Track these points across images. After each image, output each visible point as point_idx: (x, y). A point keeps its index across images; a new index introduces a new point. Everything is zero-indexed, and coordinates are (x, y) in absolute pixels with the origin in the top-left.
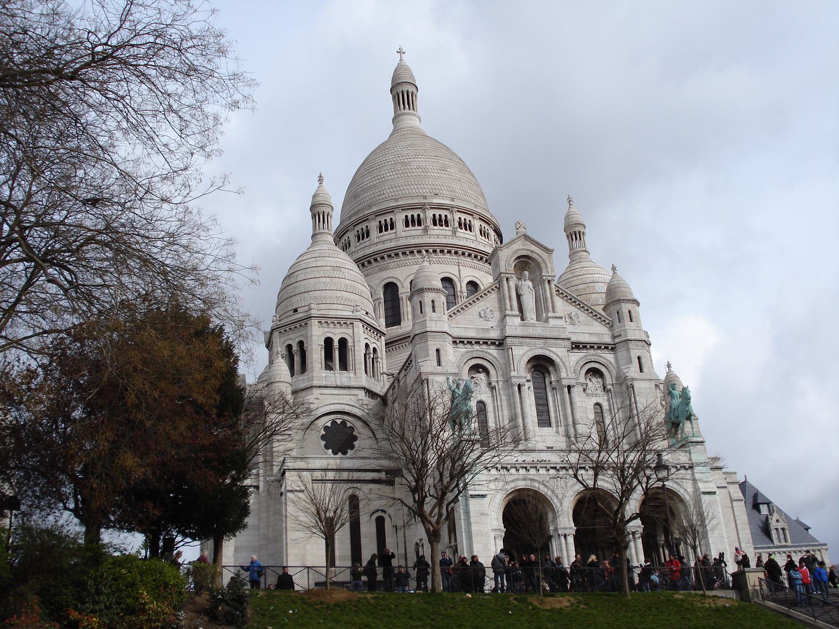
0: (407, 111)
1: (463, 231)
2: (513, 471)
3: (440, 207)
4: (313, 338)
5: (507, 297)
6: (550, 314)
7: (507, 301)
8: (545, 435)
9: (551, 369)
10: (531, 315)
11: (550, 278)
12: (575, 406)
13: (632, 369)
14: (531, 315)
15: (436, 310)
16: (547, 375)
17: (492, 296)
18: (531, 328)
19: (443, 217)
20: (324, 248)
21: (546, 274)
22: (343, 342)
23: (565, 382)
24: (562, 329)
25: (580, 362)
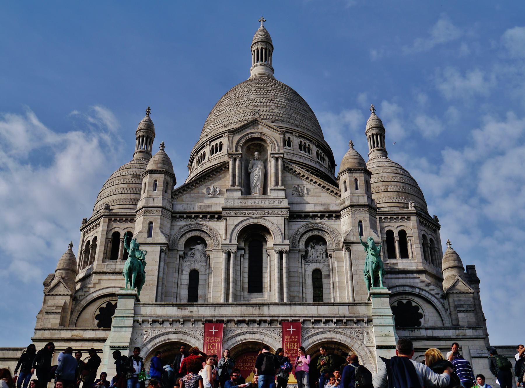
0: (259, 63)
2: (167, 325)
10: (257, 191)
11: (276, 156)
13: (352, 234)
16: (264, 244)
17: (221, 176)
18: (249, 200)
21: (274, 152)
24: (281, 200)
25: (301, 230)
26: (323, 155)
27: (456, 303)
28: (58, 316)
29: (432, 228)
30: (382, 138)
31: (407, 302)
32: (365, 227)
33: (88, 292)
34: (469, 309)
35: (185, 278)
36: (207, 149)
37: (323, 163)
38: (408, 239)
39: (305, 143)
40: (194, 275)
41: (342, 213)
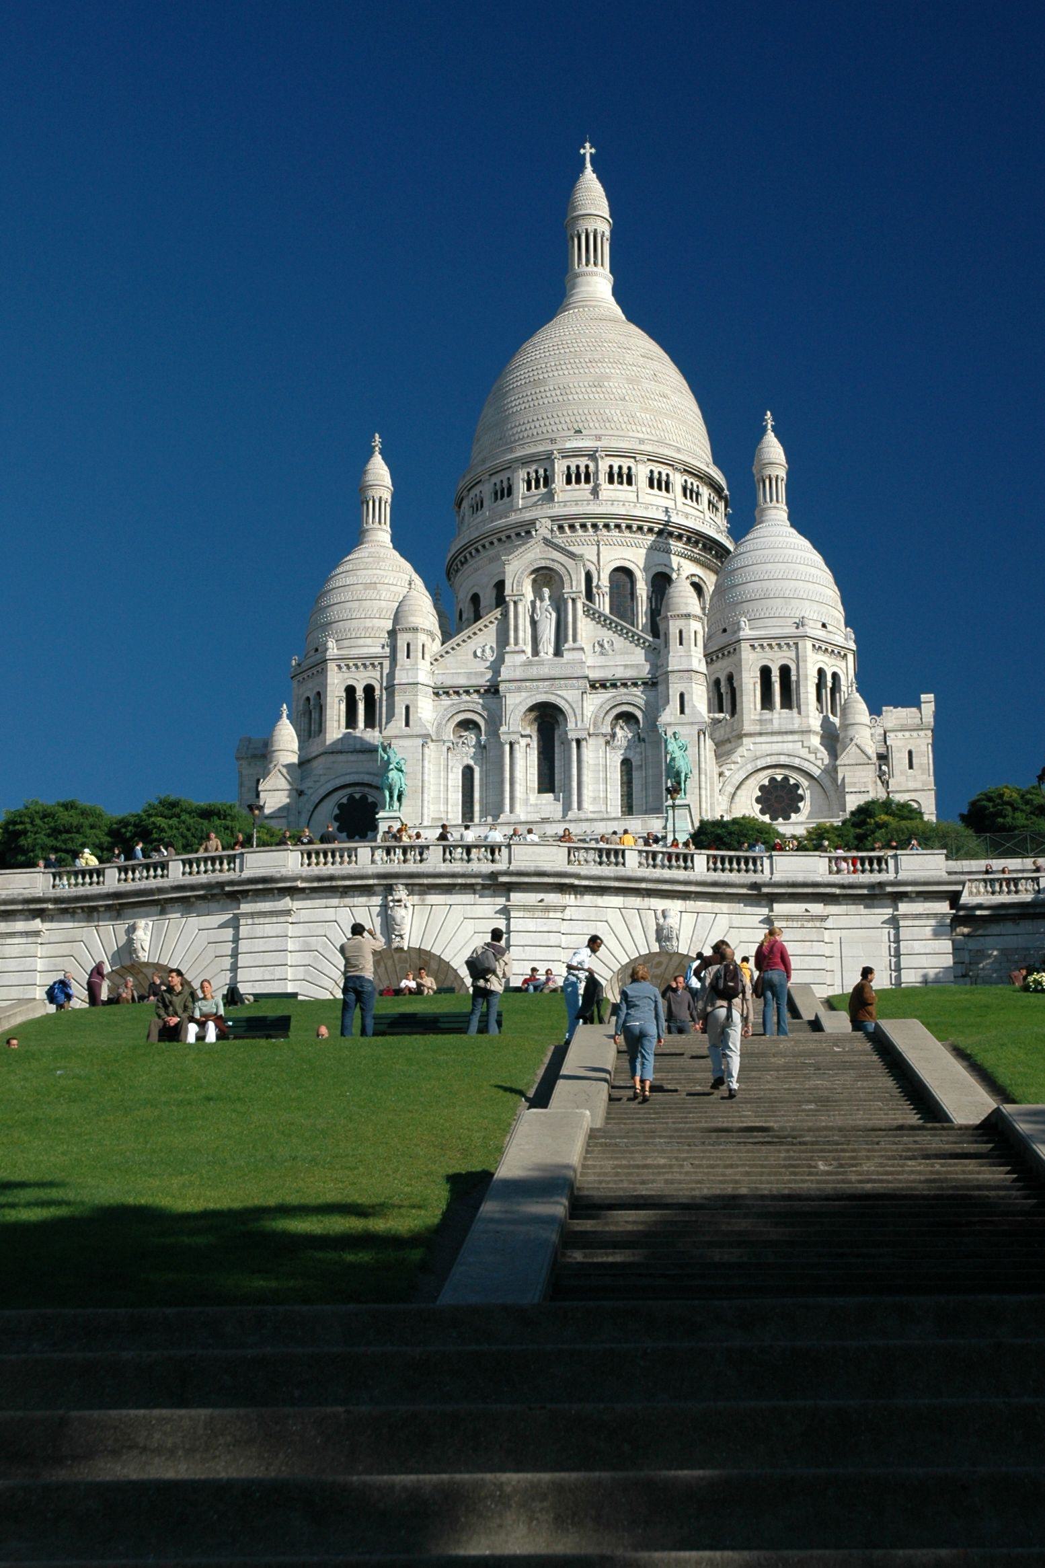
1: (616, 486)
3: (576, 453)
4: (328, 689)
5: (512, 627)
6: (570, 644)
7: (512, 633)
8: (541, 804)
9: (561, 718)
11: (573, 596)
12: (585, 765)
14: (547, 647)
15: (411, 654)
16: (556, 727)
18: (535, 668)
19: (582, 469)
20: (363, 555)
22: (369, 690)
23: (572, 735)
25: (606, 705)
26: (698, 487)
27: (846, 780)
28: (284, 820)
29: (839, 653)
30: (779, 481)
31: (783, 779)
32: (688, 701)
33: (318, 781)
34: (863, 790)
35: (456, 779)
36: (486, 489)
37: (695, 504)
38: (794, 678)
39: (660, 473)
40: (468, 772)
41: (659, 678)
